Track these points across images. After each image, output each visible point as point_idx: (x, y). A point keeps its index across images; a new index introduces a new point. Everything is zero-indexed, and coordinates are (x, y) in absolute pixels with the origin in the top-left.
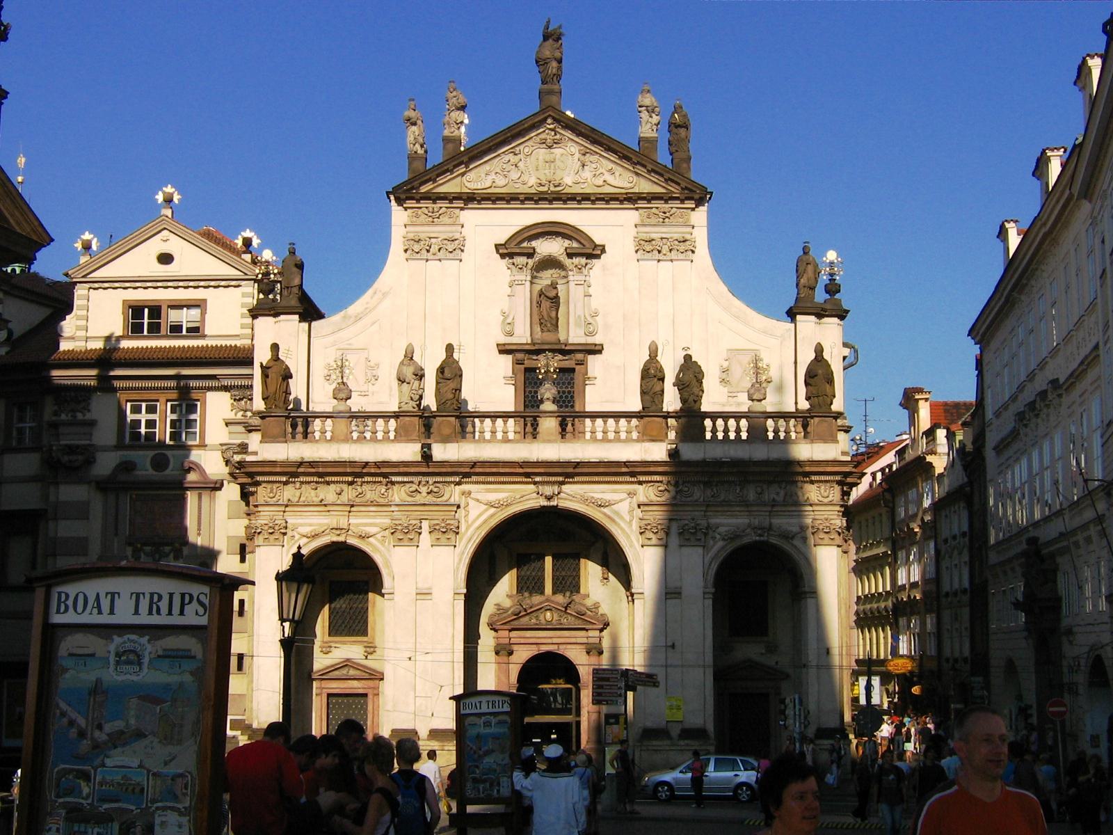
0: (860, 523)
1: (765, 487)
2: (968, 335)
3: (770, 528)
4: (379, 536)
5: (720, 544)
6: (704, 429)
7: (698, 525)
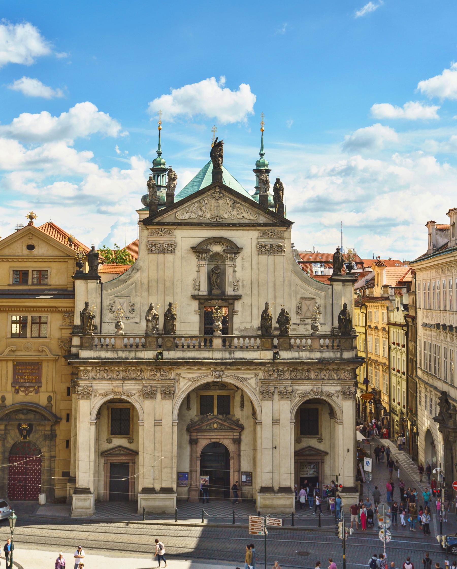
1: (319, 372)
3: (321, 392)
4: (137, 395)
5: (298, 399)
7: (287, 390)
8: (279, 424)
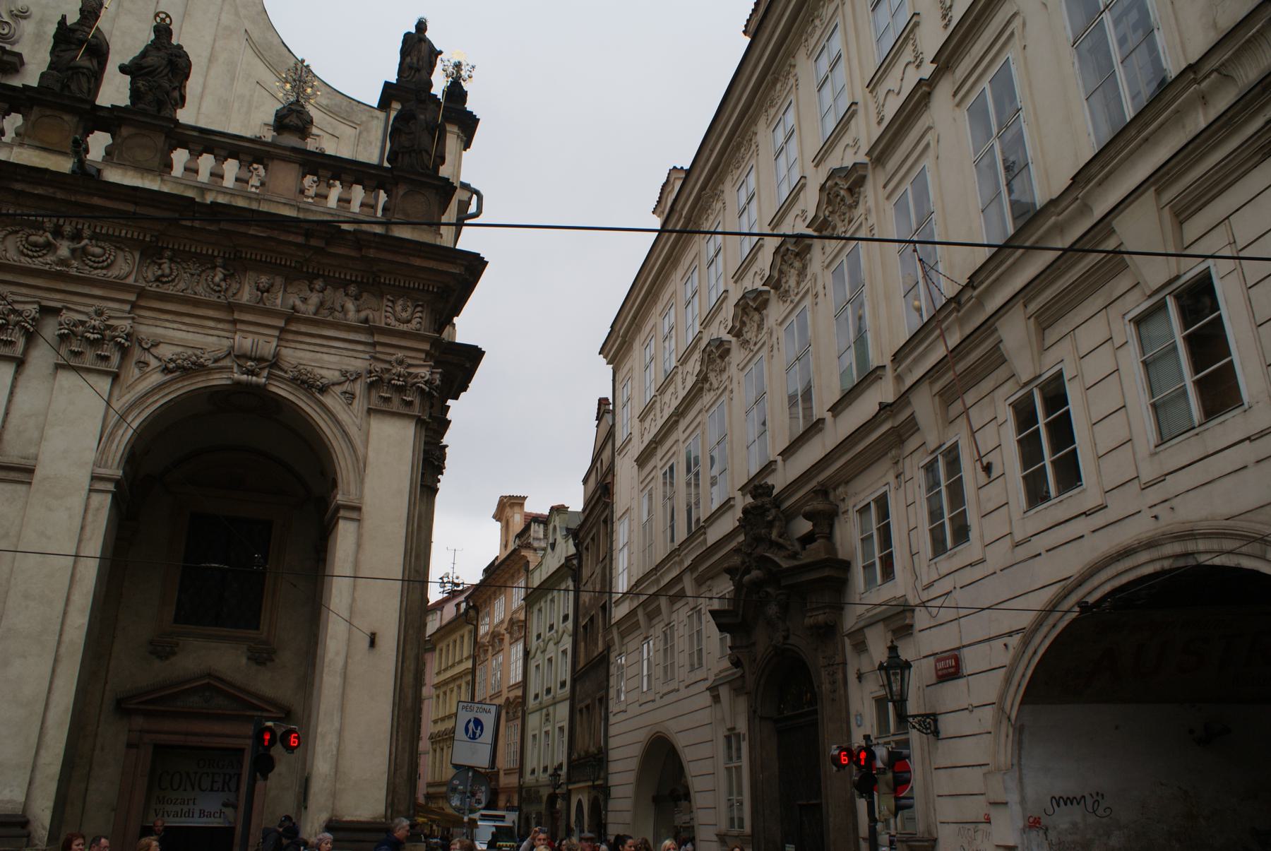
0: (441, 650)
1: (279, 281)
2: (600, 353)
3: (274, 363)
5: (156, 378)
6: (169, 166)
7: (109, 327)
8: (30, 483)
